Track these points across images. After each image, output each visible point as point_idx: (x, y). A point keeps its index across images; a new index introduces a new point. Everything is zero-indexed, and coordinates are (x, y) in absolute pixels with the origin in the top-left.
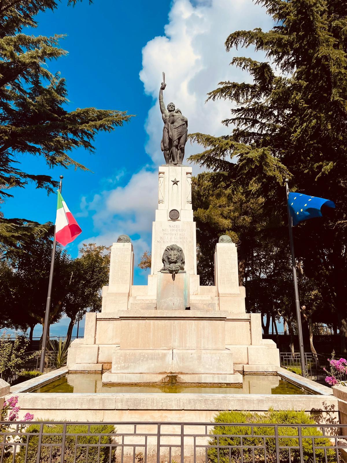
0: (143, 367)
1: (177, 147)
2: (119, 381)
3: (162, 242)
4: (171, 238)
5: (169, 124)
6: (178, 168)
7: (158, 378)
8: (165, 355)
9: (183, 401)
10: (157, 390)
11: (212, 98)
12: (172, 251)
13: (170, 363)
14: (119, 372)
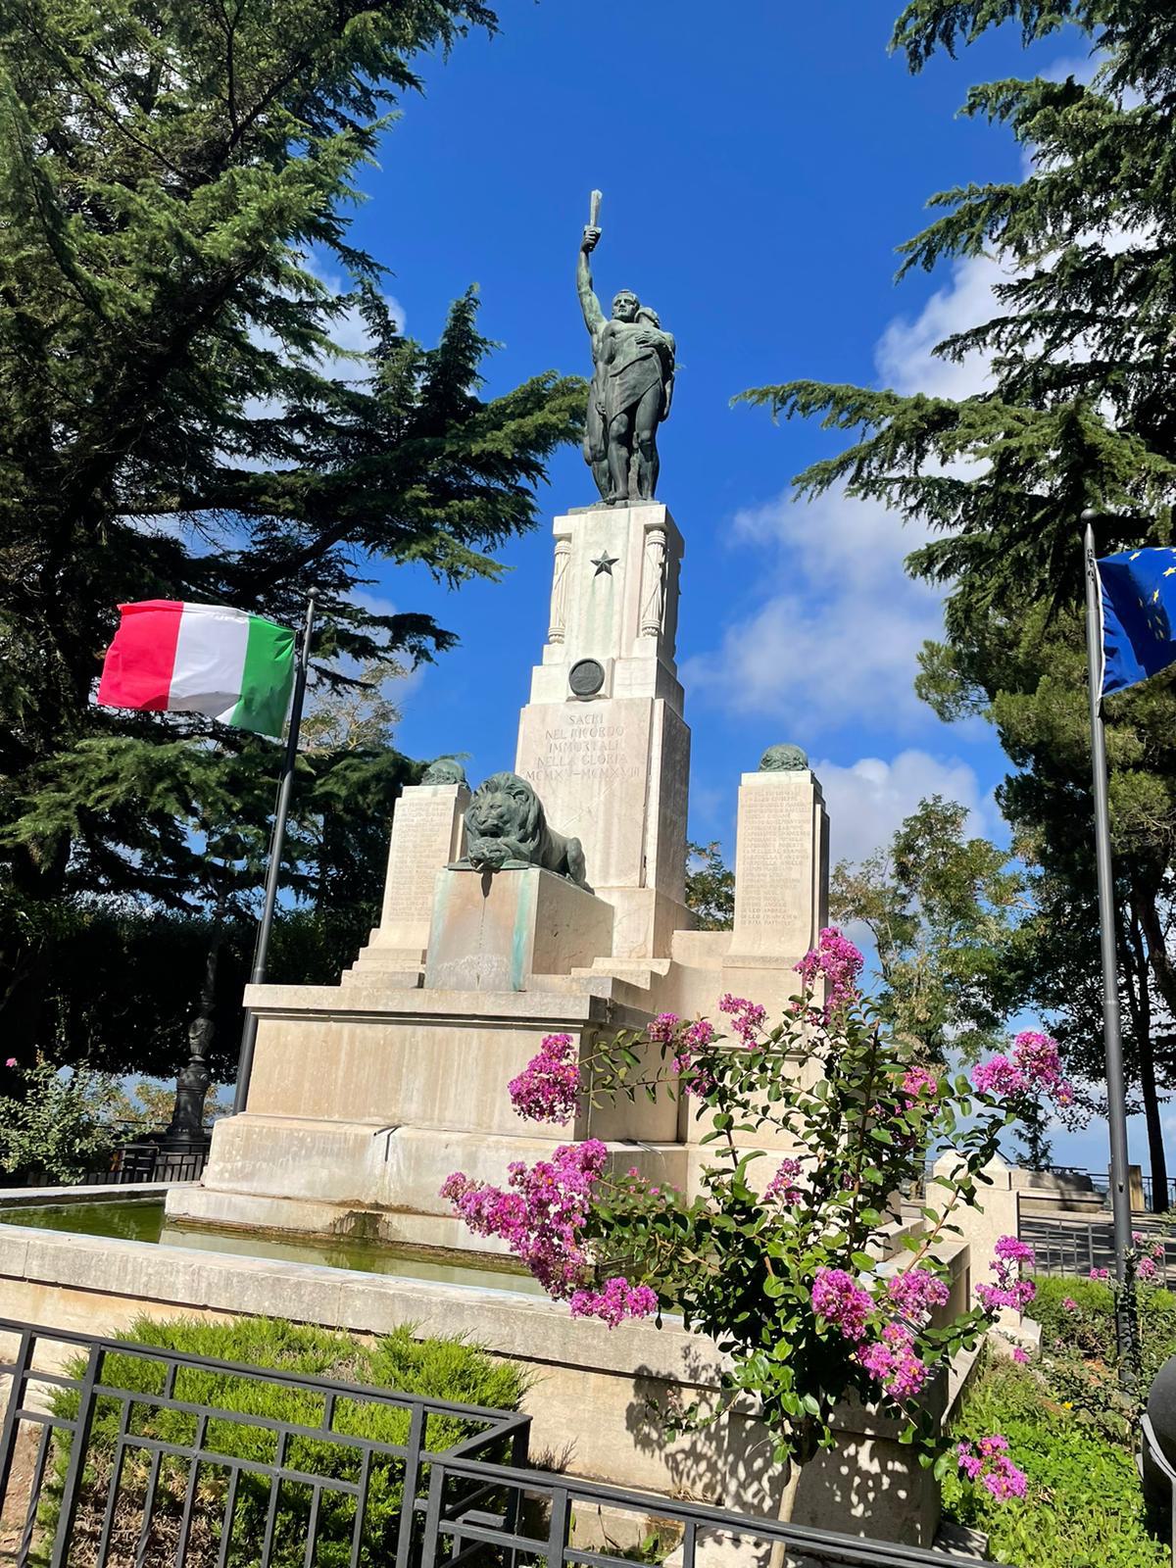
0: (294, 1180)
1: (625, 439)
2: (211, 1216)
3: (542, 776)
4: (571, 763)
5: (601, 364)
6: (619, 514)
7: (321, 1219)
8: (362, 1144)
9: (208, 1278)
10: (315, 1255)
11: (920, 260)
12: (490, 795)
13: (377, 1171)
14: (224, 1186)
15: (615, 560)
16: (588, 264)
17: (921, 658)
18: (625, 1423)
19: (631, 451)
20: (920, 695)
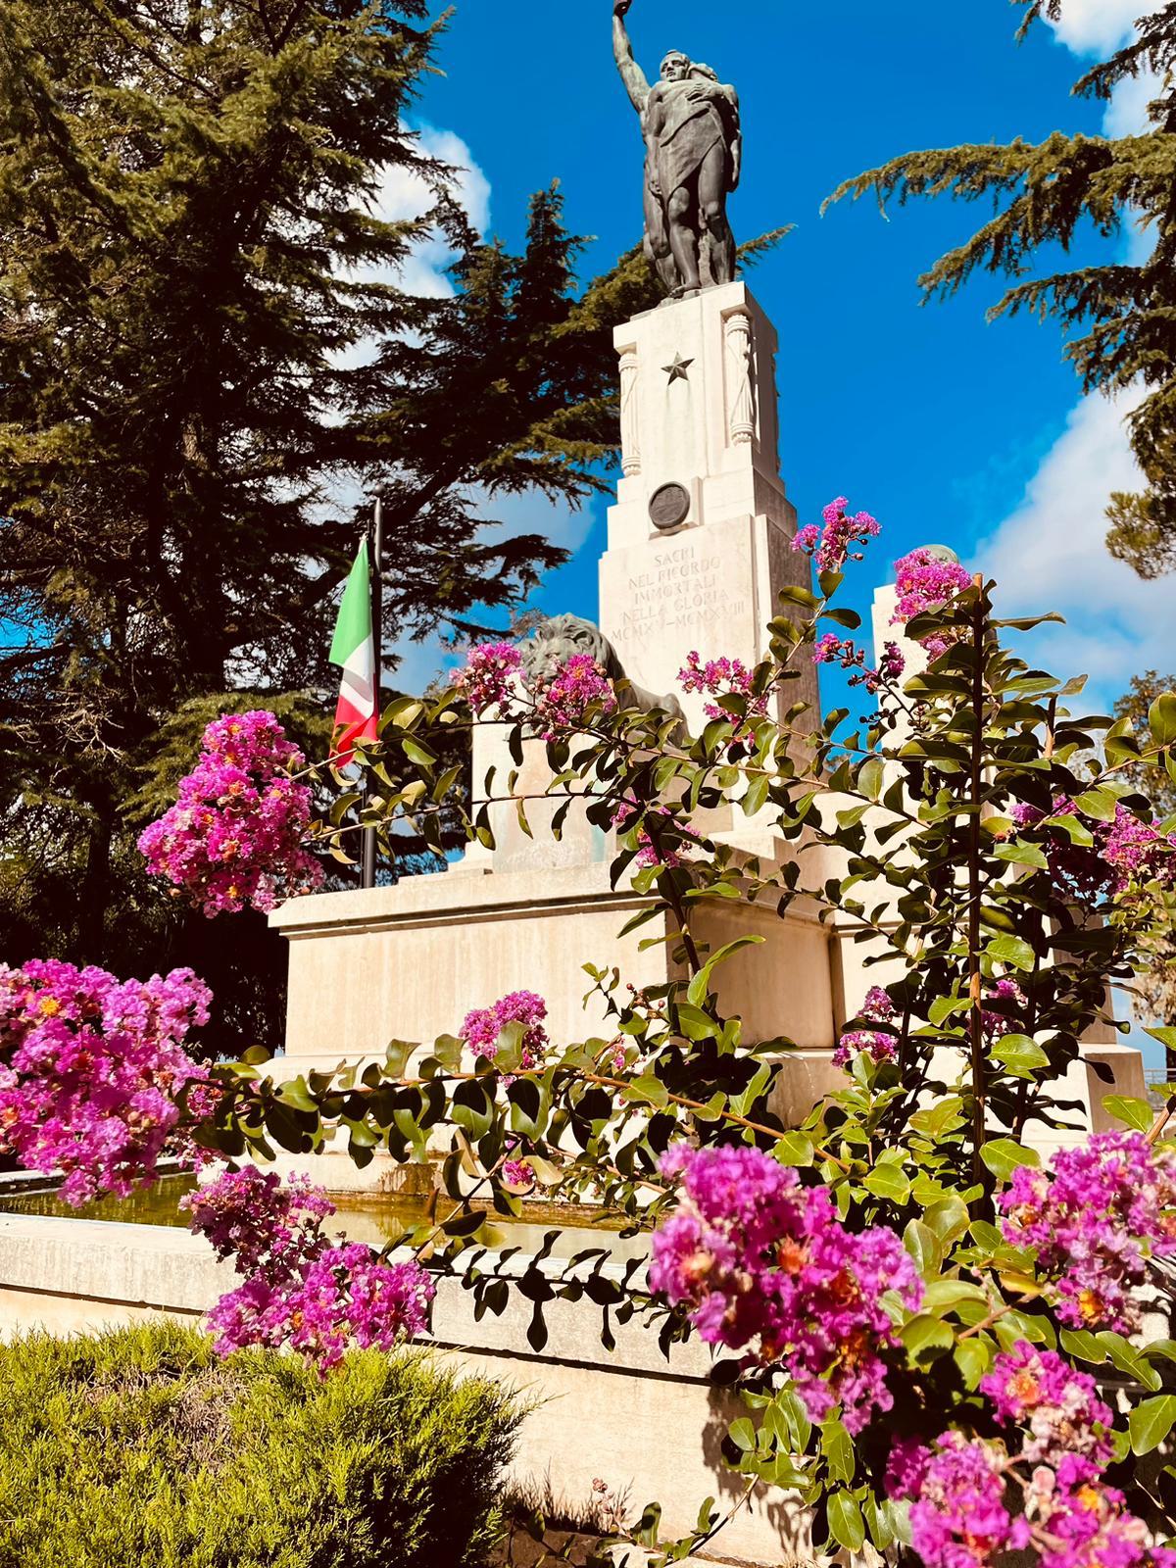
1: (688, 219)
3: (630, 633)
12: (545, 643)
15: (688, 362)
16: (624, 29)
17: (1110, 513)
18: (701, 1457)
19: (698, 233)
20: (1114, 554)
